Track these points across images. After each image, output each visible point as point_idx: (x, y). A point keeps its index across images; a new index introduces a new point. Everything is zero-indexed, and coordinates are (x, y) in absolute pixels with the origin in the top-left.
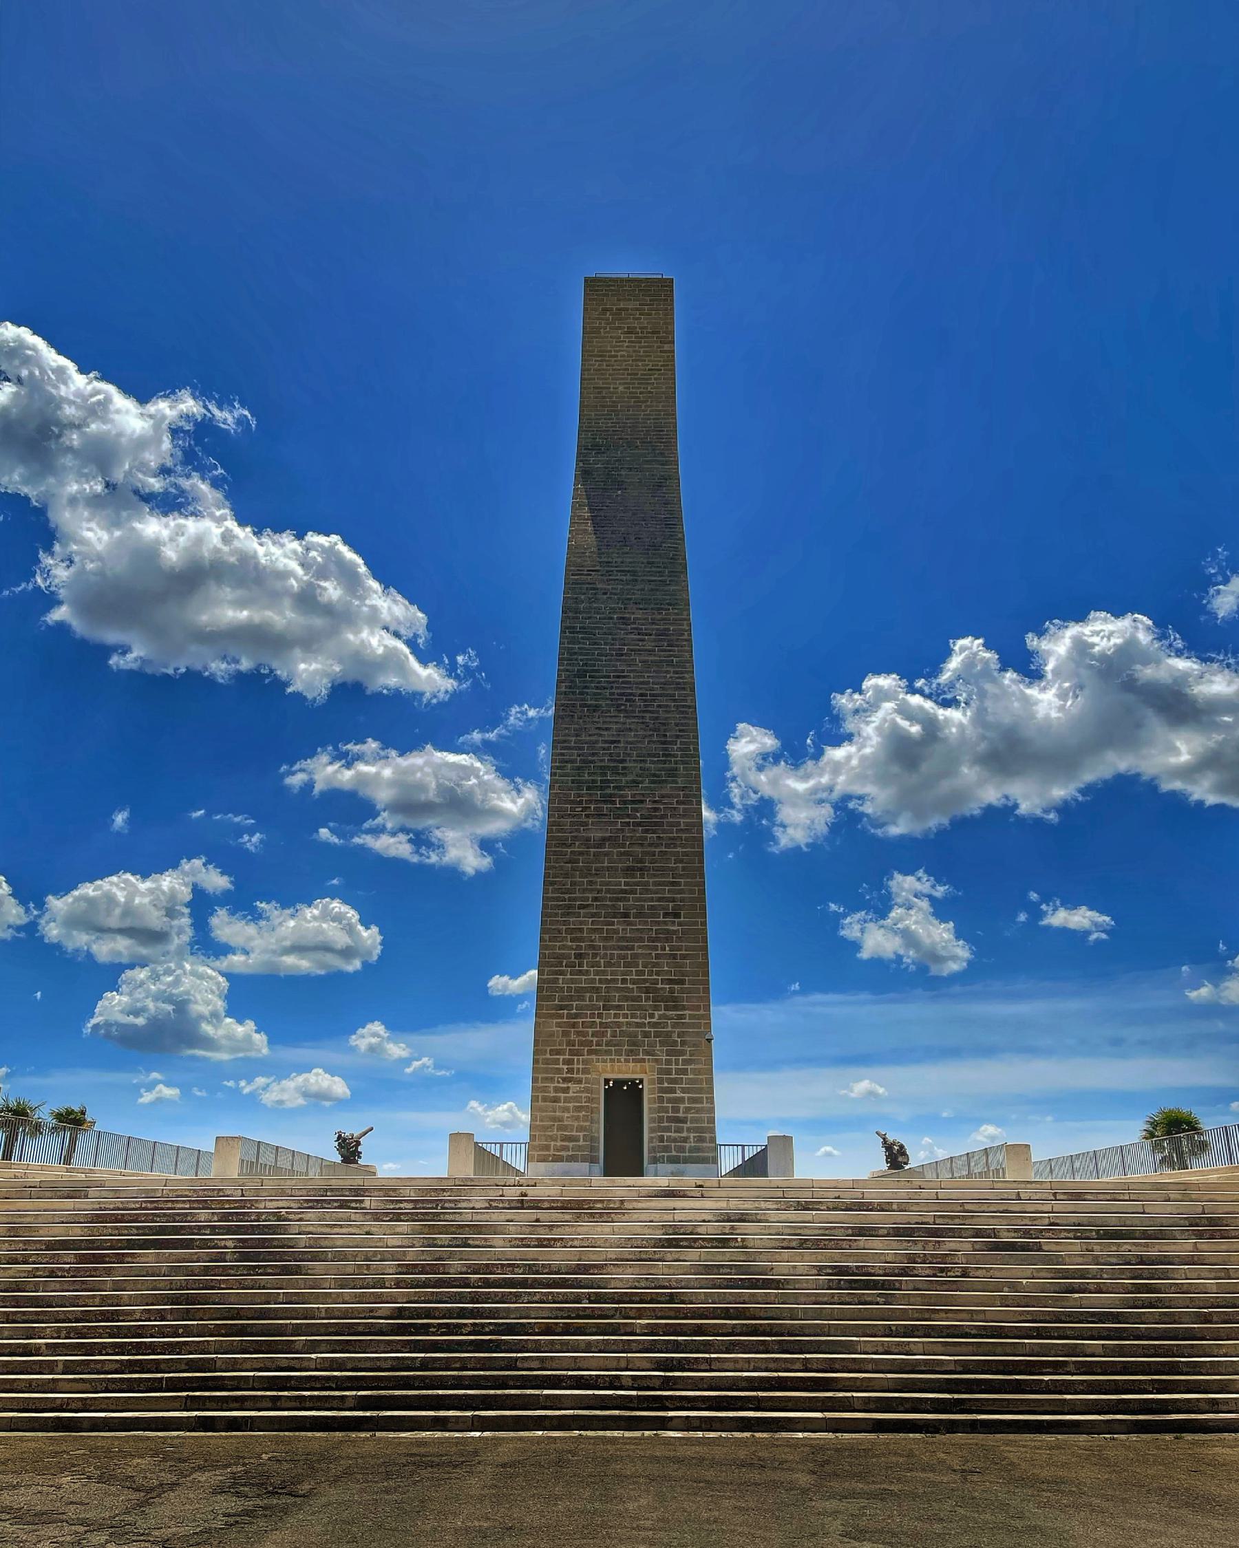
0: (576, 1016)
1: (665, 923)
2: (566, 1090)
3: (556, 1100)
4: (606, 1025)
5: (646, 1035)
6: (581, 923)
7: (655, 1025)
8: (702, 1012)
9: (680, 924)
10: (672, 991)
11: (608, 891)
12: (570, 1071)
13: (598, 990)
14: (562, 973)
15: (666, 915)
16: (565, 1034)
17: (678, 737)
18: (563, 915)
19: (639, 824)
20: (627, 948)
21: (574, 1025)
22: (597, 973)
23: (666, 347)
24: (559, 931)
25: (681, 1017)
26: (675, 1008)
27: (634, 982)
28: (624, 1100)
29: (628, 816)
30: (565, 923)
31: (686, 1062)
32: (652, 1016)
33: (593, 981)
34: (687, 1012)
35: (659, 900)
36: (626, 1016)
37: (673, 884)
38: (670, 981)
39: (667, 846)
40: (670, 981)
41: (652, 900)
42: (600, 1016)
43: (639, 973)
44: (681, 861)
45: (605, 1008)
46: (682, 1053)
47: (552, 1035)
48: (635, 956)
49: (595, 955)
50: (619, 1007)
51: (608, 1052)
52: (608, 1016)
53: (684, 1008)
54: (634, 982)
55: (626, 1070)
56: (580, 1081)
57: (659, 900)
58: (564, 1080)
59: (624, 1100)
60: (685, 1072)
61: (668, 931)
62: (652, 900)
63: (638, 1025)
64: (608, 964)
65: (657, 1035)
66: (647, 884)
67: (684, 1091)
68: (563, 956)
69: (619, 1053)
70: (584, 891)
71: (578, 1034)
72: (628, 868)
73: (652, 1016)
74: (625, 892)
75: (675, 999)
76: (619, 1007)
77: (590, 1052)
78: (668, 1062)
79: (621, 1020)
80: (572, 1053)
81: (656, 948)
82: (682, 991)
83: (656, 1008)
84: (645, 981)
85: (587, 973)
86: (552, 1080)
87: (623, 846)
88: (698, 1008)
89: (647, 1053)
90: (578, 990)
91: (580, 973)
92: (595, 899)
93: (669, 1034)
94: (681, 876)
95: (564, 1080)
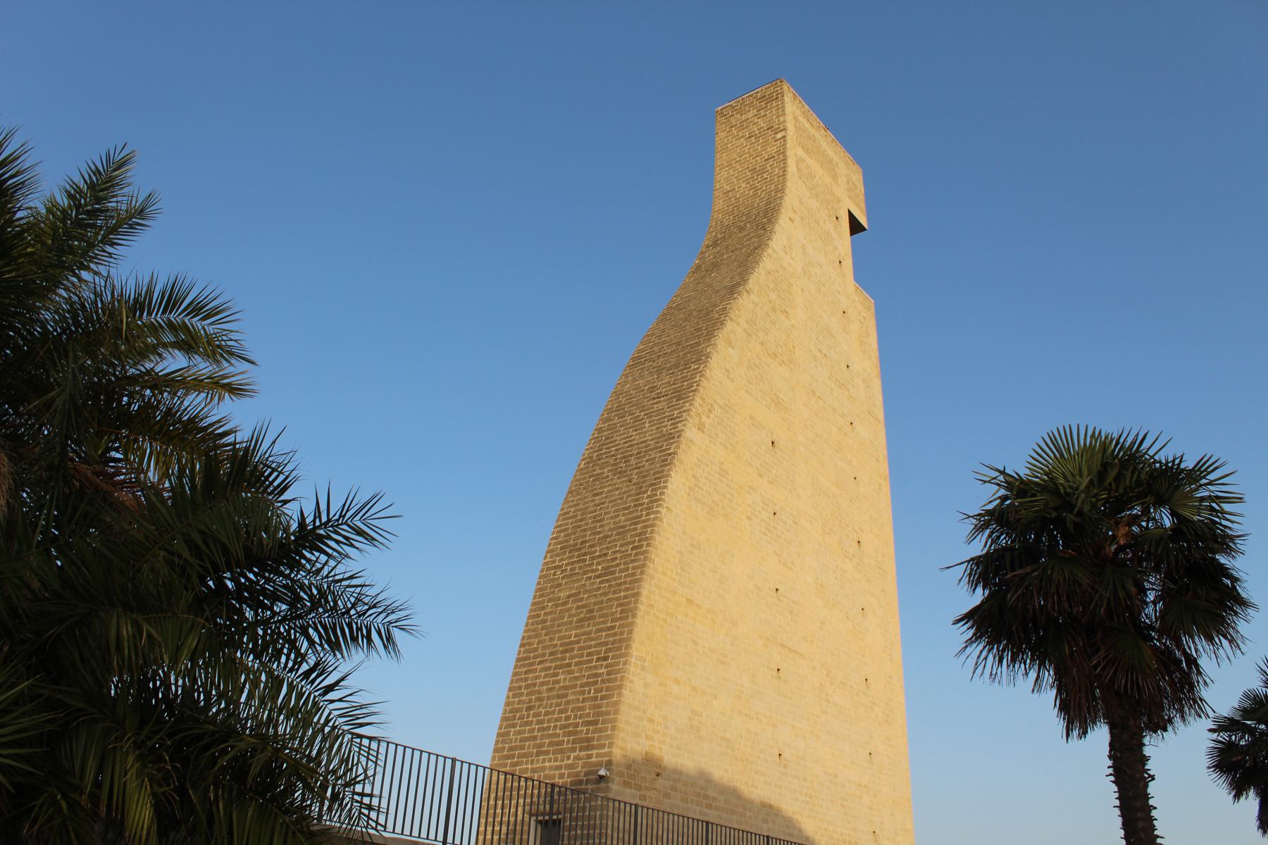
8: (606, 750)
9: (607, 667)
10: (588, 731)
13: (535, 738)
15: (598, 660)
17: (651, 485)
23: (779, 136)
25: (590, 756)
26: (588, 748)
27: (562, 727)
29: (592, 571)
32: (569, 758)
33: (532, 731)
34: (595, 752)
36: (550, 760)
39: (615, 592)
41: (590, 647)
43: (568, 718)
44: (621, 605)
45: (538, 754)
48: (568, 703)
50: (547, 753)
53: (593, 747)
54: (562, 727)
61: (596, 675)
62: (590, 647)
64: (547, 714)
66: (590, 633)
68: (517, 710)
70: (544, 648)
72: (581, 620)
75: (588, 740)
76: (547, 753)
79: (547, 764)
81: (583, 693)
82: (594, 732)
83: (573, 750)
84: (570, 725)
88: (603, 746)
91: (527, 724)
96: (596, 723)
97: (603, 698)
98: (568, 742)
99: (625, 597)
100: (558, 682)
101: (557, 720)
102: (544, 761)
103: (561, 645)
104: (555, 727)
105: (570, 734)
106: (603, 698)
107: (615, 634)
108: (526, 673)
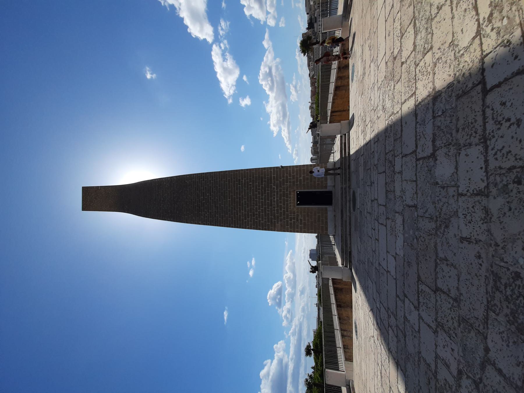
0: (274, 216)
1: (242, 184)
2: (301, 220)
3: (305, 224)
4: (277, 205)
5: (280, 190)
6: (243, 214)
7: (277, 187)
10: (265, 181)
11: (232, 205)
12: (294, 219)
13: (265, 208)
14: (260, 221)
16: (281, 221)
18: (240, 221)
19: (210, 194)
20: (251, 198)
21: (278, 217)
22: (259, 209)
24: (246, 222)
27: (262, 196)
28: (304, 198)
30: (243, 220)
31: (290, 176)
32: (274, 188)
35: (234, 187)
37: (229, 182)
38: (262, 182)
40: (262, 182)
41: (234, 189)
42: (274, 208)
44: (222, 179)
46: (287, 176)
47: (281, 225)
49: (253, 210)
51: (287, 204)
52: (274, 204)
53: (271, 177)
54: (262, 196)
55: (293, 197)
56: (298, 215)
57: (234, 187)
58: (297, 220)
59: (304, 198)
60: (293, 176)
61: (245, 183)
62: (234, 189)
63: (277, 194)
64: (256, 205)
65: (281, 187)
67: (300, 176)
69: (287, 201)
71: (281, 216)
73: (274, 188)
74: (232, 200)
77: (287, 211)
78: (290, 182)
80: (287, 218)
85: (259, 212)
86: (298, 226)
87: (217, 199)
89: (287, 191)
90: (265, 216)
91: (259, 215)
92: (235, 210)
93: (280, 182)
94: (227, 179)
95: (297, 220)
96: (262, 178)
97: (253, 178)
98: (268, 190)
99: (219, 178)
100: (245, 202)
101: (259, 199)
102: (274, 201)
103: (232, 205)
104: (262, 199)
105: (265, 191)
106: (253, 178)
107: (231, 178)
108: (240, 221)
